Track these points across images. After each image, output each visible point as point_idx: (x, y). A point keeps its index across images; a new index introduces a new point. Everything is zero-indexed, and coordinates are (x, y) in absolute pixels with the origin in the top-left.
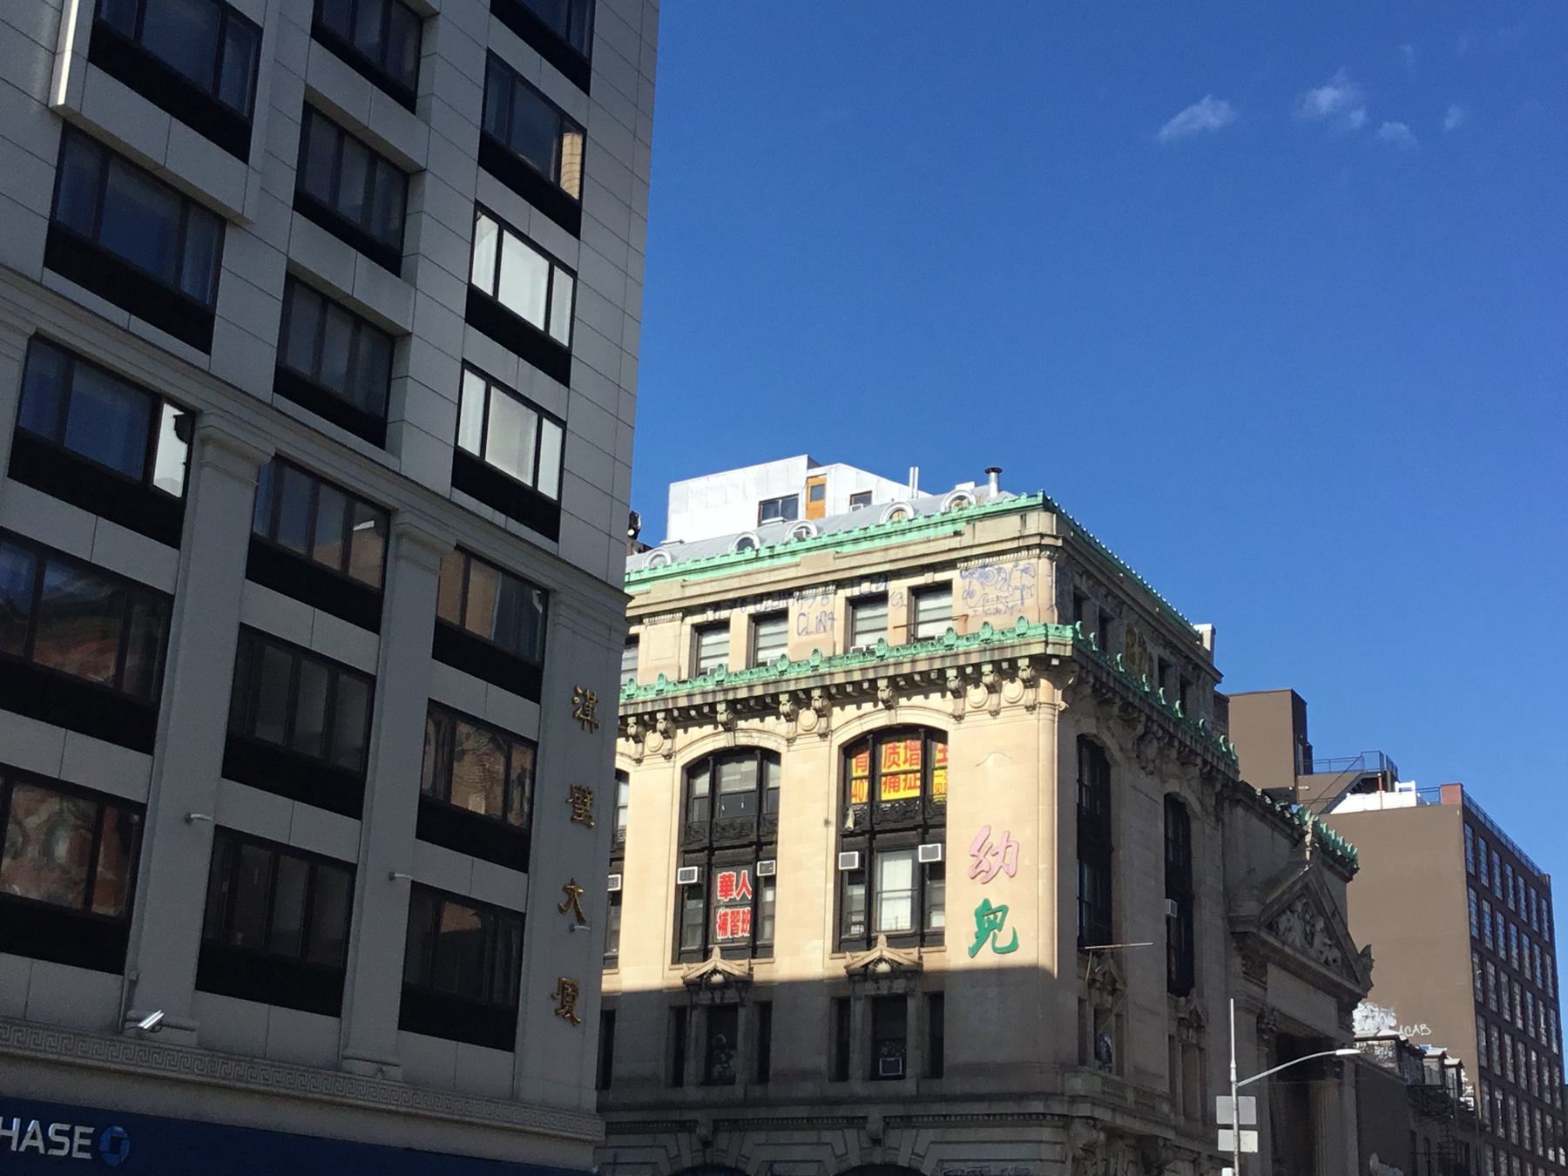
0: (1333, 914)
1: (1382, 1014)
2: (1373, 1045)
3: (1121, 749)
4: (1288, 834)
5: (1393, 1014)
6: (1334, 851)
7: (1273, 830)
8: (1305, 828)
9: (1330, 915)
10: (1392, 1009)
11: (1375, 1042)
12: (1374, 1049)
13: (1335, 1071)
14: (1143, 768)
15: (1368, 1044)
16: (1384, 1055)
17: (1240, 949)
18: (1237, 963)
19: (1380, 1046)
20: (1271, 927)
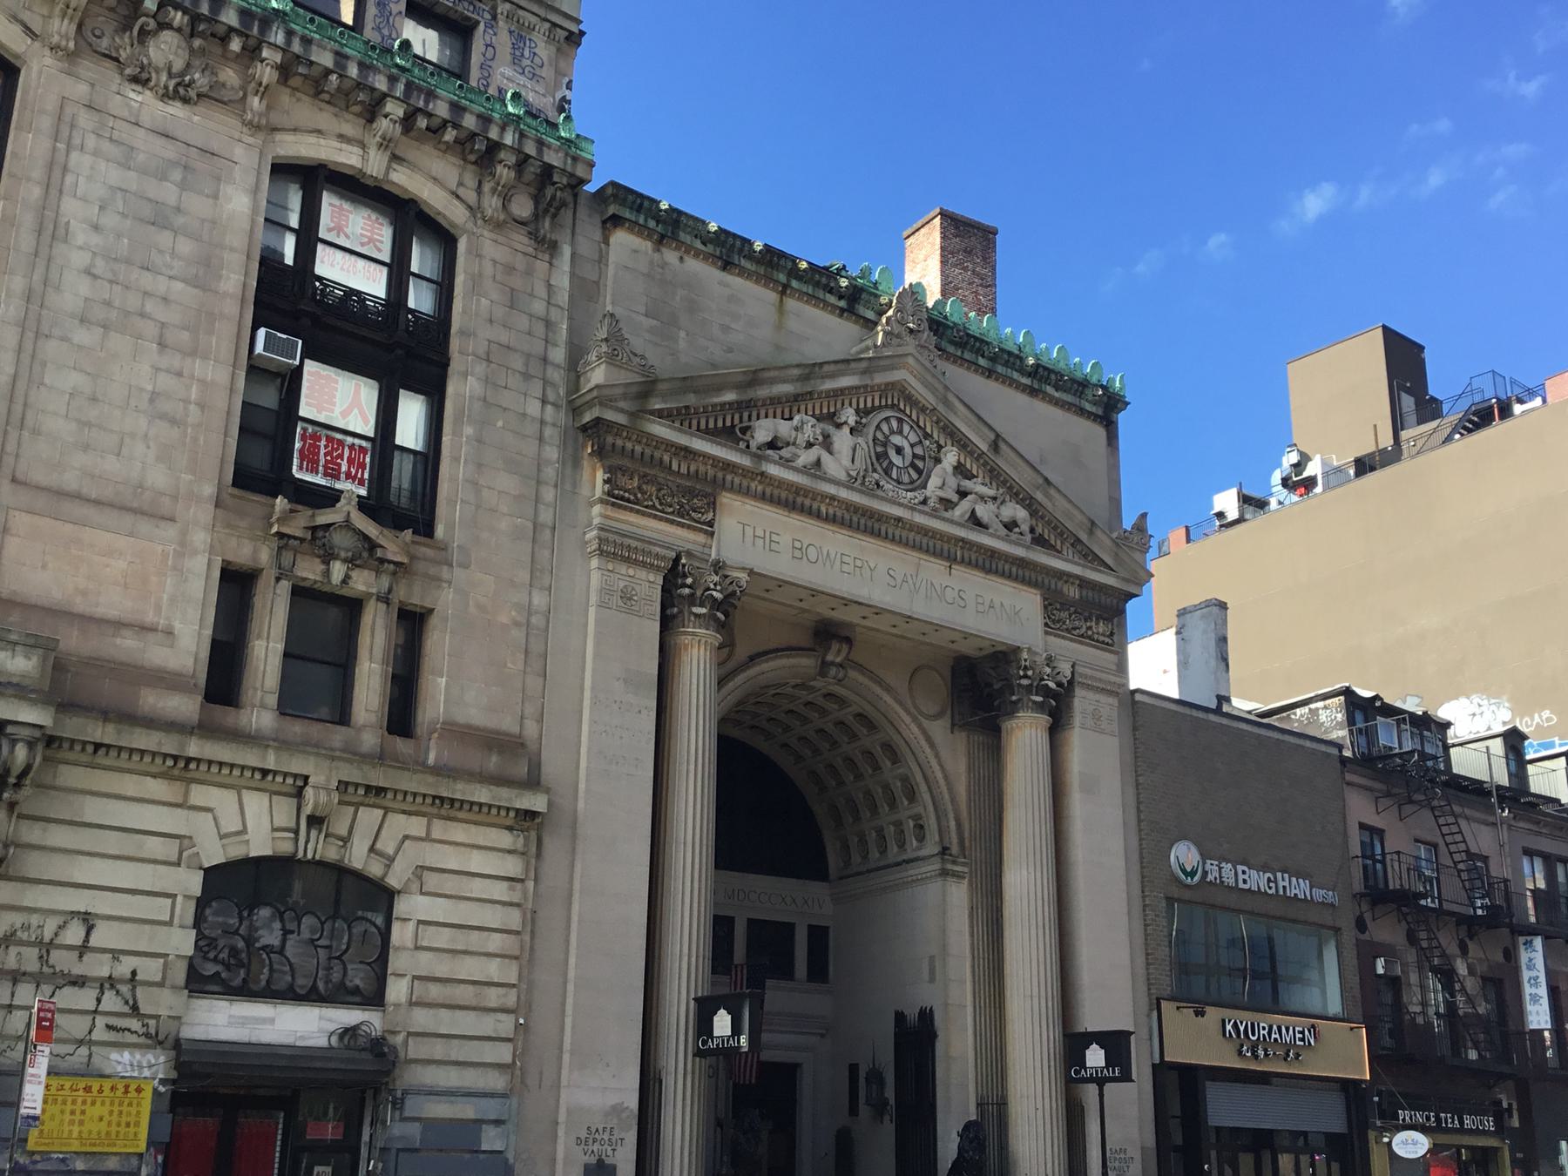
0: (995, 446)
1: (1493, 707)
2: (1317, 709)
3: (28, 30)
4: (842, 310)
5: (1507, 705)
6: (1021, 359)
7: (783, 293)
8: (884, 300)
9: (984, 447)
10: (1505, 698)
11: (1320, 704)
12: (1318, 716)
13: (1035, 702)
14: (139, 80)
15: (1310, 709)
16: (1332, 720)
17: (600, 453)
18: (596, 479)
19: (1325, 708)
20: (732, 434)
